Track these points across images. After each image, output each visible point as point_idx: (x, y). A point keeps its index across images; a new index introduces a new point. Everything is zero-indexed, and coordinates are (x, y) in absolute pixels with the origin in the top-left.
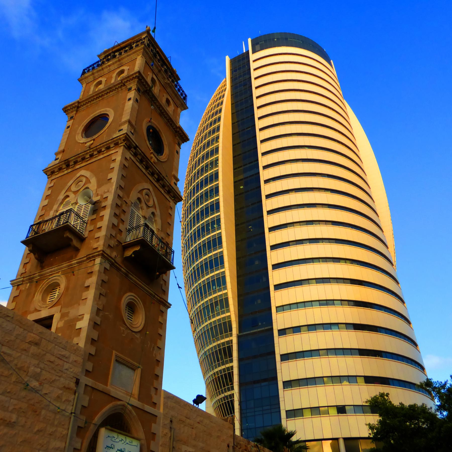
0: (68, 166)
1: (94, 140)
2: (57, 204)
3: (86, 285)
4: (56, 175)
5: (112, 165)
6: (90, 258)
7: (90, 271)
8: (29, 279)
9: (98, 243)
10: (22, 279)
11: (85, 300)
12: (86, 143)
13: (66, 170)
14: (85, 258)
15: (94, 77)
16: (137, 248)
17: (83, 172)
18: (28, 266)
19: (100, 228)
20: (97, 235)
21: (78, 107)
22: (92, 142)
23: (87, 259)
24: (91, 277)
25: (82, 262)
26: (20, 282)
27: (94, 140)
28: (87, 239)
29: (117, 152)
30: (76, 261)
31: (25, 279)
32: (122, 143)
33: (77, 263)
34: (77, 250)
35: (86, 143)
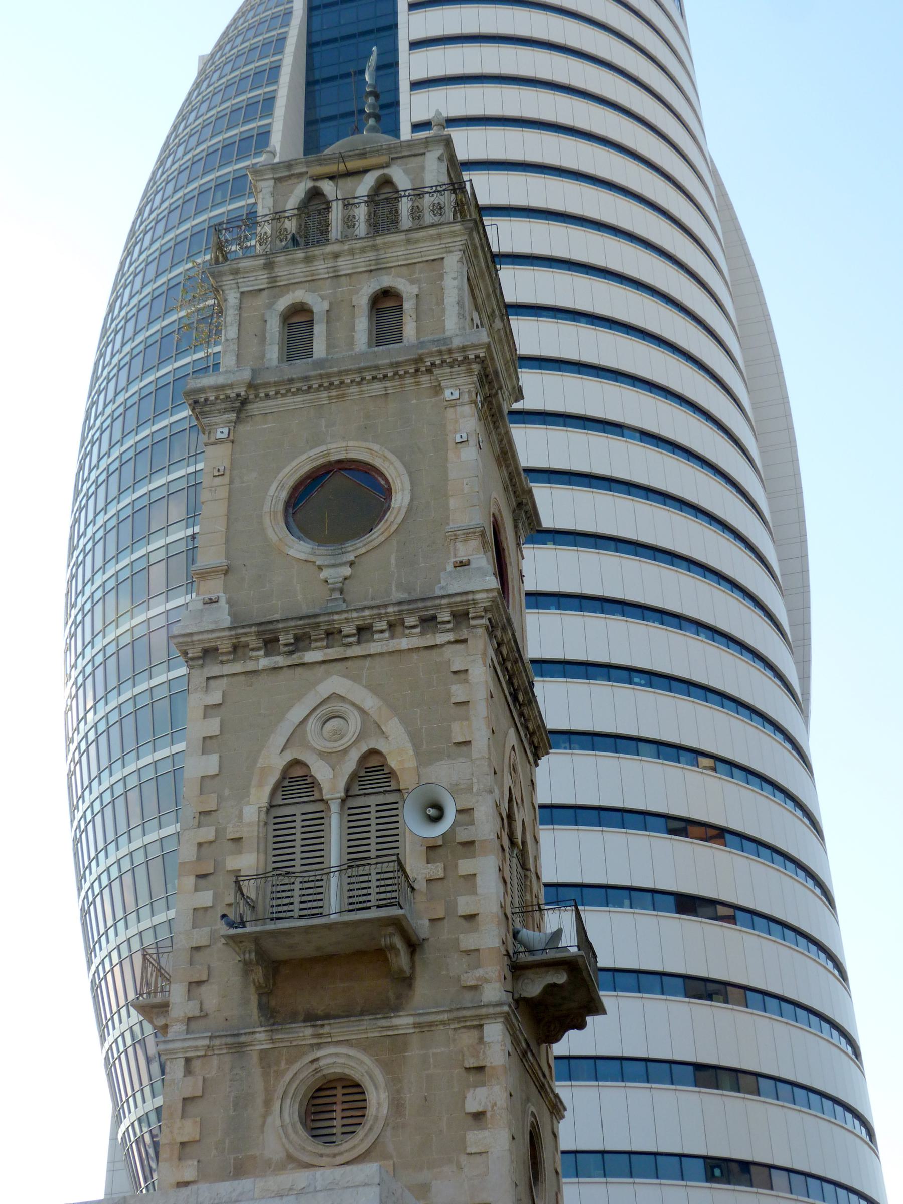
0: (270, 643)
1: (352, 564)
2: (261, 785)
3: (472, 1106)
4: (222, 662)
5: (458, 692)
6: (464, 1019)
7: (471, 1062)
8: (230, 1046)
9: (480, 972)
10: (206, 1042)
11: (479, 1159)
12: (320, 568)
13: (267, 654)
14: (445, 1017)
15: (273, 280)
16: (561, 978)
17: (335, 683)
18: (211, 997)
19: (471, 917)
20: (468, 941)
21: (245, 402)
22: (347, 571)
23: (458, 1020)
24: (483, 1084)
25: (431, 1024)
26: (196, 1048)
27: (352, 564)
28: (426, 944)
29: (464, 641)
30: (411, 1020)
31: (217, 1042)
32: (482, 617)
33: (416, 1025)
34: (406, 981)
35: (320, 568)
